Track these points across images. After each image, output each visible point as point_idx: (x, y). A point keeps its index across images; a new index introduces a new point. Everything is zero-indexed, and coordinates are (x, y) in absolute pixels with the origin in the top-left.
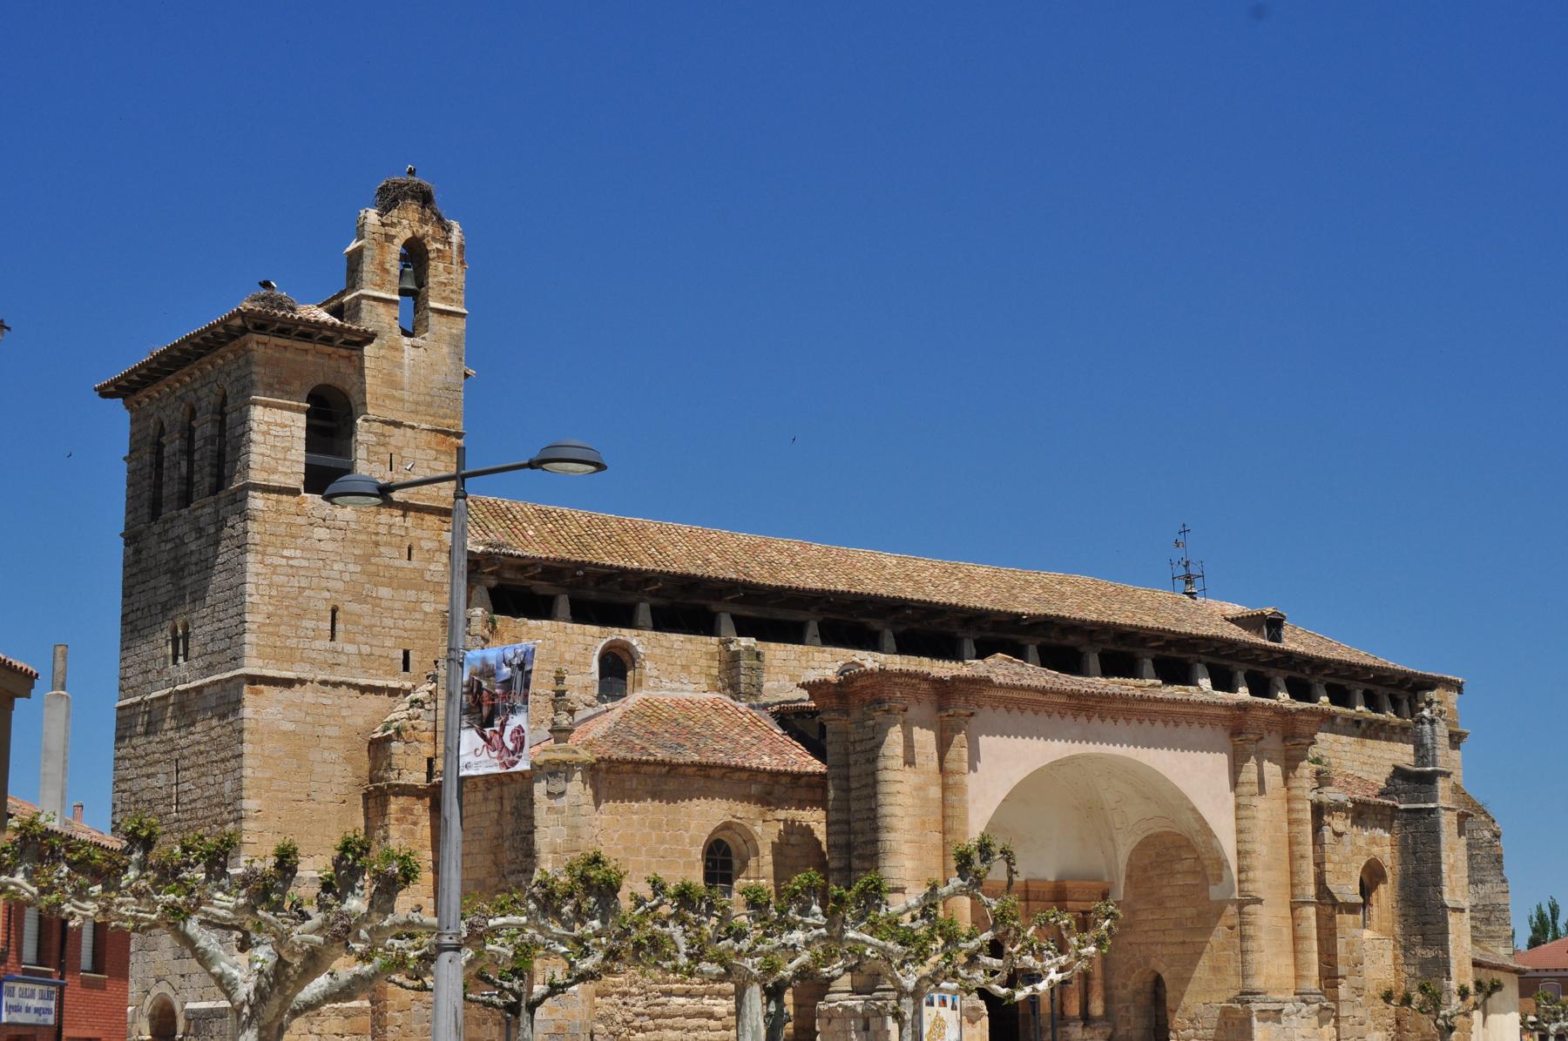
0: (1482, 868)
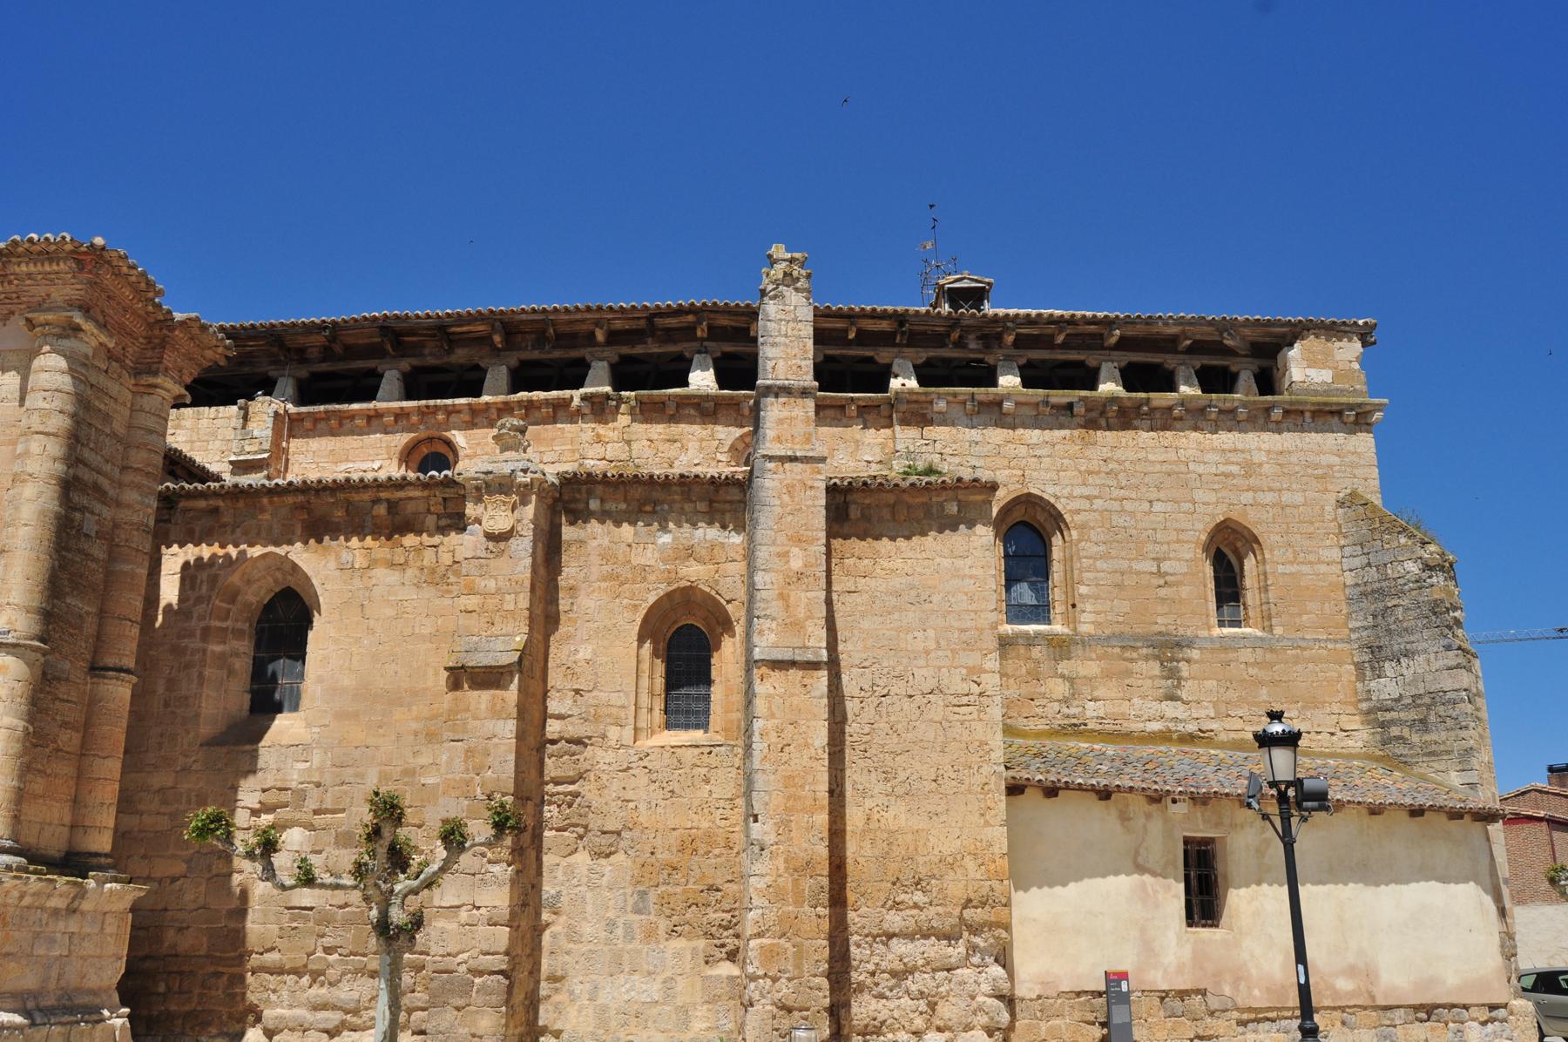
0: (1406, 630)
